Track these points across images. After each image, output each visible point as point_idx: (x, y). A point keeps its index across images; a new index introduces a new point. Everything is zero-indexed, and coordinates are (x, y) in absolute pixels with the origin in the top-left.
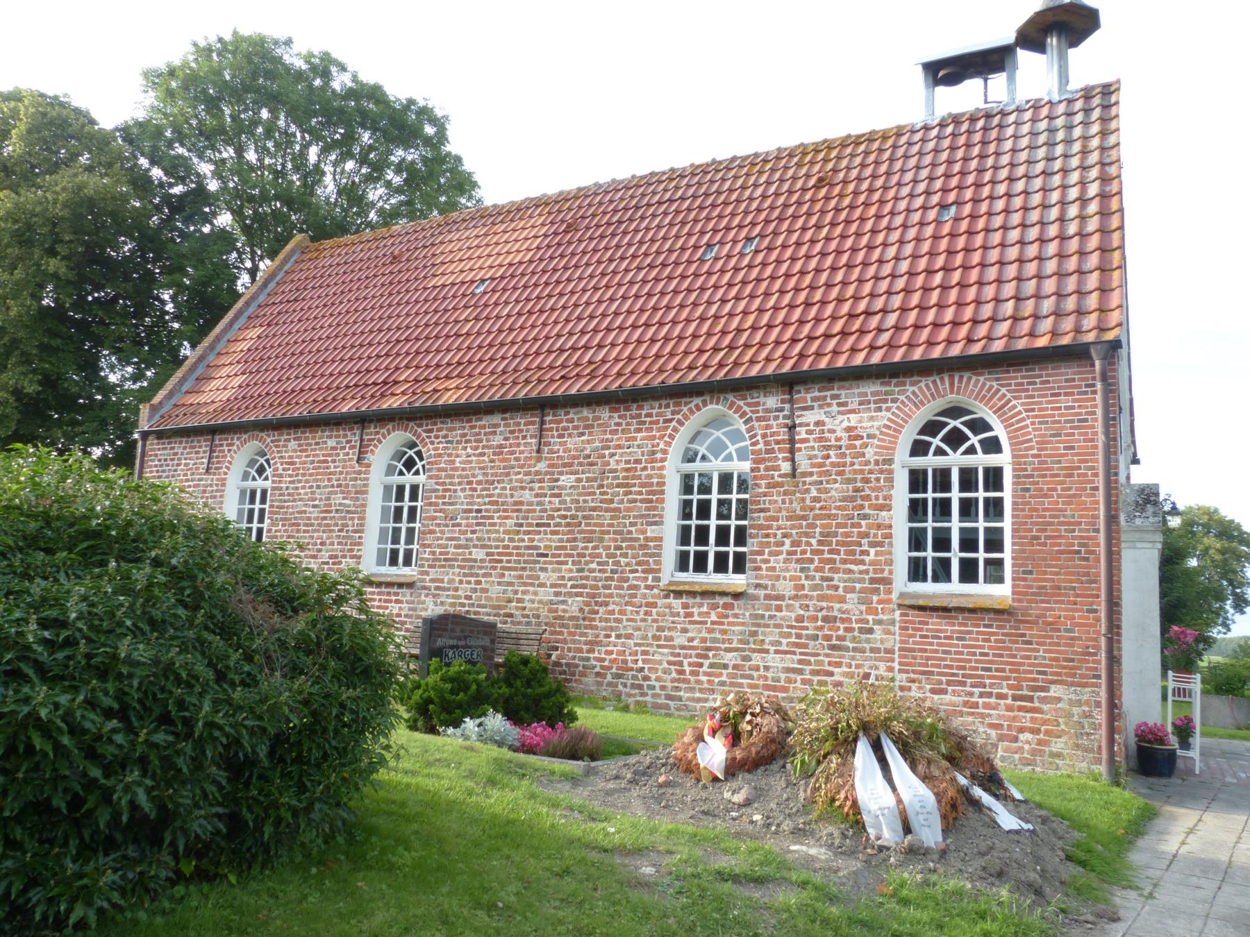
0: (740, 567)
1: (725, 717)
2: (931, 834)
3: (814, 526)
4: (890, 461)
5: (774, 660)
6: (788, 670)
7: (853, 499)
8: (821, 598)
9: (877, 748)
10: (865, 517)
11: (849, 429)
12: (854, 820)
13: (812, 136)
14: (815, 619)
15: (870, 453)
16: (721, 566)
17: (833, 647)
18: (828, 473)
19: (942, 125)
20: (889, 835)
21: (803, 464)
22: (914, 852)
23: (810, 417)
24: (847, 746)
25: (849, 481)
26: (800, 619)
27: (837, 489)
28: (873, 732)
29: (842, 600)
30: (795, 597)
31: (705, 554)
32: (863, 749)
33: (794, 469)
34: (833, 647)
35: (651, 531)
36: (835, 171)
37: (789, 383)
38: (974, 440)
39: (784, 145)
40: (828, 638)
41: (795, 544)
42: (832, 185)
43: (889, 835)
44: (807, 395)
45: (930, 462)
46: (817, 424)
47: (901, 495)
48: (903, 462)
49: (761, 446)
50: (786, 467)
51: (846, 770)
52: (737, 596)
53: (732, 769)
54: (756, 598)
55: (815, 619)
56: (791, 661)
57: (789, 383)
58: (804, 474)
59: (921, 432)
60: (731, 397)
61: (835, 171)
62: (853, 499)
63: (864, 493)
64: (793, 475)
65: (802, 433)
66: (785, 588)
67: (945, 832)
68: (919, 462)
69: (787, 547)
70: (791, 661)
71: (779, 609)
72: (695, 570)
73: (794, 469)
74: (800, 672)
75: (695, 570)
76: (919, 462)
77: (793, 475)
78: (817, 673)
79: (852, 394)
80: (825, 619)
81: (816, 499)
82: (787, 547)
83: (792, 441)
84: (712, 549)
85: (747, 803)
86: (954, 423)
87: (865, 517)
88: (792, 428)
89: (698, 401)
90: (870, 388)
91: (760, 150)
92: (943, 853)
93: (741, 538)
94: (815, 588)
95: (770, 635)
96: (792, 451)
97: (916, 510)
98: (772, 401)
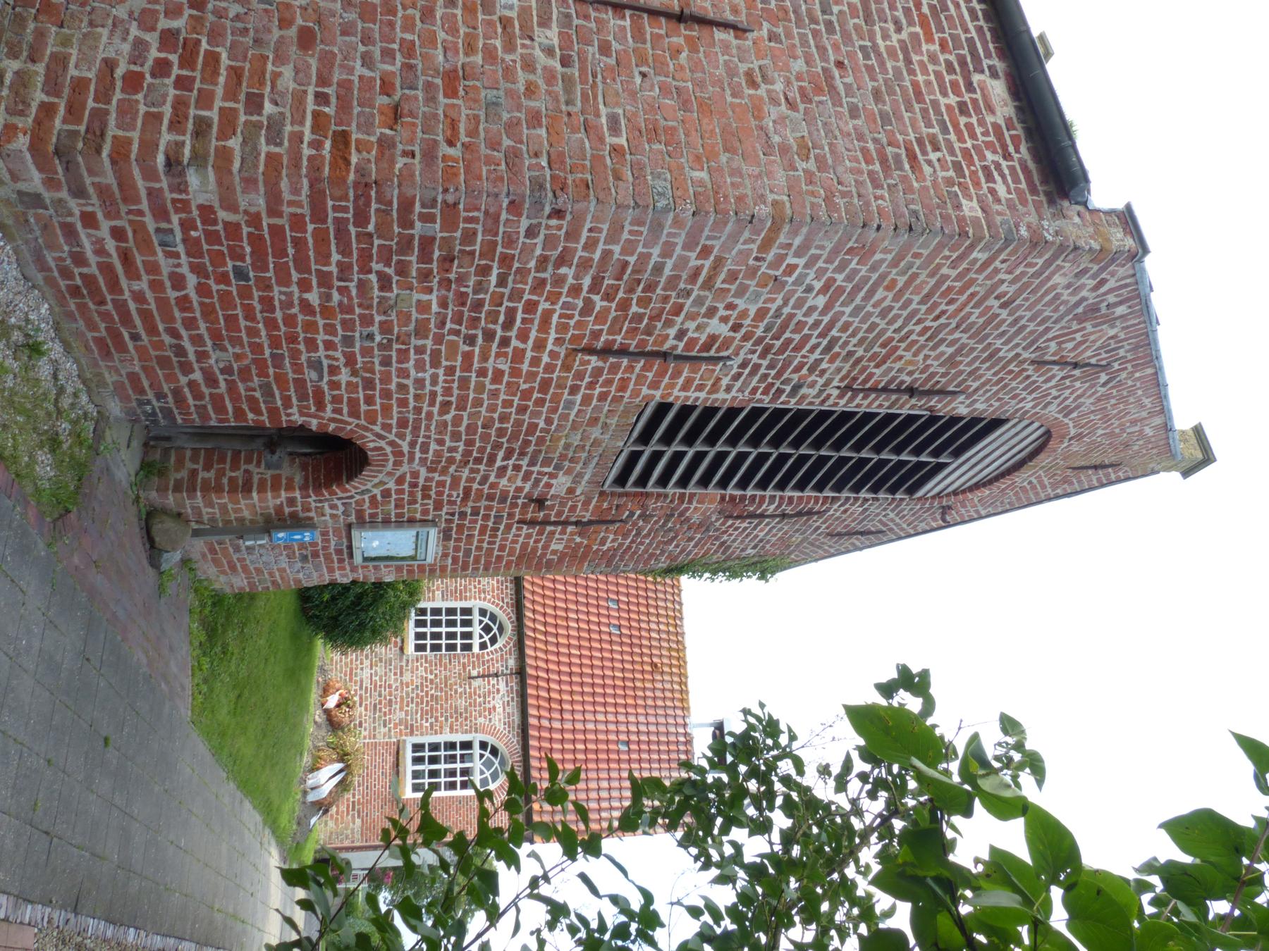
0: (420, 648)
1: (347, 699)
2: (311, 798)
3: (441, 690)
4: (476, 731)
5: (367, 673)
6: (362, 681)
7: (456, 712)
8: (402, 698)
9: (340, 771)
10: (446, 720)
11: (494, 708)
12: (314, 768)
13: (690, 655)
14: (390, 694)
15: (481, 720)
16: (420, 636)
17: (375, 706)
18: (470, 697)
19: (686, 734)
20: (310, 783)
21: (476, 683)
22: (305, 793)
23: (502, 686)
24: (341, 760)
25: (466, 709)
26: (390, 686)
27: (462, 703)
28: (347, 769)
29: (401, 709)
30: (402, 683)
31: (425, 626)
32: (340, 766)
33: (473, 678)
34: (375, 706)
35: (438, 594)
36: (662, 673)
37: (521, 673)
38: (487, 774)
39: (686, 637)
40: (380, 703)
41: (432, 681)
42: (652, 673)
43: (310, 783)
44: (514, 684)
45: (477, 751)
46: (498, 690)
47: (458, 738)
48: (477, 738)
49: (487, 657)
50: (474, 673)
51: (332, 761)
52: (402, 649)
53: (327, 712)
54: (401, 660)
55: (390, 694)
56: (367, 683)
57: (521, 673)
58: (470, 684)
59: (493, 747)
60: (515, 638)
61: (662, 673)
62: (456, 712)
63: (459, 717)
64: (470, 678)
65: (493, 681)
66: (407, 677)
67: (312, 803)
68: (476, 745)
69: (430, 677)
70: (367, 683)
71: (395, 674)
72: (414, 785)
73: (473, 678)
74: (361, 688)
75: (414, 772)
76: (476, 745)
77: (470, 678)
78: (361, 698)
79: (514, 709)
80: (390, 701)
81: (456, 691)
82: (430, 677)
83: (489, 676)
84: (428, 630)
85: (316, 723)
86: (496, 762)
87: (446, 720)
88: (496, 675)
89: (514, 618)
90: (516, 719)
91: (685, 621)
92: (304, 803)
93: (436, 648)
94: (408, 694)
95: (380, 670)
96: (483, 676)
97: (451, 746)
98: (512, 663)
